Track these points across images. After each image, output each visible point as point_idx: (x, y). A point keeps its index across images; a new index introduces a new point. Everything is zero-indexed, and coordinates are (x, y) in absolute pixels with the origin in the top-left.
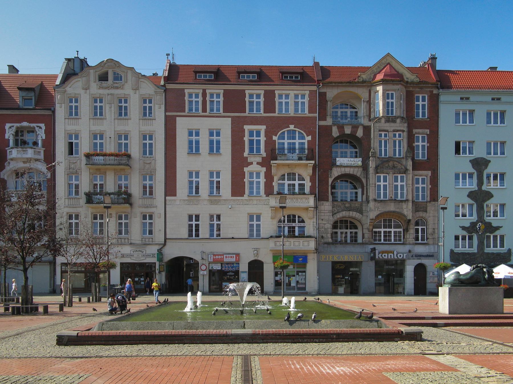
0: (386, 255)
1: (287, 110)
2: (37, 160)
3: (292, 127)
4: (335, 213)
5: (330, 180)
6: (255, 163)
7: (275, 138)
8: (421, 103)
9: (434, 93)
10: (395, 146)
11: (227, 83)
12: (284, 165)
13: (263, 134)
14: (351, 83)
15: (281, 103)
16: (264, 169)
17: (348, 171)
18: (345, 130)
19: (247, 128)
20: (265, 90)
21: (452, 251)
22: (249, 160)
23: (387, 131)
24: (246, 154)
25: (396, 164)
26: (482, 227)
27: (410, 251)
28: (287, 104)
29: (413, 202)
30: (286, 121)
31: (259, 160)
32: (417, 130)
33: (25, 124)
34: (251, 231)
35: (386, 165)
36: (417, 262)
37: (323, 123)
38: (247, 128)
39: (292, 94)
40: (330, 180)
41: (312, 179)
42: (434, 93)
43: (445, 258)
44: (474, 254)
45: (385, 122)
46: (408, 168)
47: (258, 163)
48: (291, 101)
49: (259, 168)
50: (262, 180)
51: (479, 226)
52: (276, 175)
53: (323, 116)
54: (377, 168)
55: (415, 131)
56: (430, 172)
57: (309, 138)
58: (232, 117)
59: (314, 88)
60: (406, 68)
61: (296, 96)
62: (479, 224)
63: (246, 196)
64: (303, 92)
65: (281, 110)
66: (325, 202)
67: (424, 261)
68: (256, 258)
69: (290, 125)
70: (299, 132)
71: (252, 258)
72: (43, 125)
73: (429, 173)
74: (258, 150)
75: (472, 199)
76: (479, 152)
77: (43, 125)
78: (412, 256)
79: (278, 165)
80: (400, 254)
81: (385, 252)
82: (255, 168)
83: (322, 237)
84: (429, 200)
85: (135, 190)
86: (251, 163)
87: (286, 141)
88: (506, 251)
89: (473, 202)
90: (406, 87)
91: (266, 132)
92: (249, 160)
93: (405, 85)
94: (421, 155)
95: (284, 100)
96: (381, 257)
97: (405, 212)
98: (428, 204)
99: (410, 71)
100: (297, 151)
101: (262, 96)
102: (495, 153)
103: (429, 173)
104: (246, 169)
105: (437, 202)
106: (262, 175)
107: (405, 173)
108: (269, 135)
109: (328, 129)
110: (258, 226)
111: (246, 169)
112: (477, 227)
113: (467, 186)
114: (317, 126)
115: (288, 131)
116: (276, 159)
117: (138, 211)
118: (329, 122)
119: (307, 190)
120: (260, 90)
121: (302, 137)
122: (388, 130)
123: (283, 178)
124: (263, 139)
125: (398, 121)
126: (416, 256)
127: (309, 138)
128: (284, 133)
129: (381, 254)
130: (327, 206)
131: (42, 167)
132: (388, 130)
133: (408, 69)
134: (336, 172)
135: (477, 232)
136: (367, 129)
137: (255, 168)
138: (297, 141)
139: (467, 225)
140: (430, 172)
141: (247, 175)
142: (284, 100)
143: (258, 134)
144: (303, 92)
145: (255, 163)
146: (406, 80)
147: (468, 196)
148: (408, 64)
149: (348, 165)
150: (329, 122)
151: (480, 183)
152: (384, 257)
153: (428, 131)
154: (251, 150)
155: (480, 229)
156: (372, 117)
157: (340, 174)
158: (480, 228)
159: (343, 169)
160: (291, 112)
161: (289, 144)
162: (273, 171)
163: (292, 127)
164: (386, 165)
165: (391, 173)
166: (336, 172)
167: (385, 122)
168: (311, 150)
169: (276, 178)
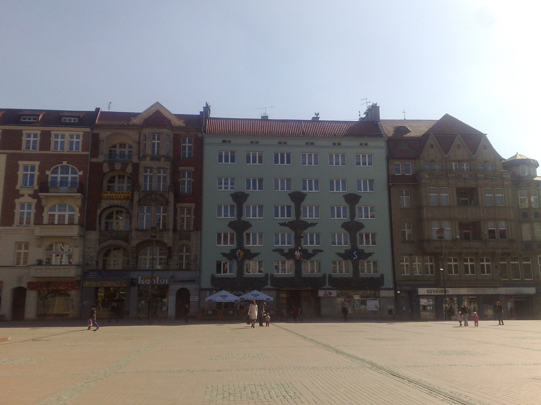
0: (149, 280)
1: (62, 148)
3: (65, 163)
4: (101, 242)
5: (99, 212)
6: (26, 195)
7: (48, 173)
8: (187, 145)
9: (199, 136)
10: (159, 181)
11: (19, 125)
12: (55, 197)
13: (37, 168)
14: (122, 127)
15: (56, 142)
16: (35, 201)
17: (116, 202)
18: (116, 166)
19: (21, 163)
20: (84, 132)
21: (213, 277)
22: (21, 193)
23: (152, 168)
24: (18, 187)
25: (159, 197)
26: (242, 254)
27: (172, 277)
28: (62, 143)
29: (175, 229)
30: (60, 158)
31: (31, 192)
32: (182, 167)
34: (19, 259)
35: (149, 198)
36: (180, 286)
37: (94, 160)
38: (21, 163)
39: (67, 134)
40: (99, 212)
41: (81, 211)
42: (199, 136)
43: (206, 283)
44: (233, 279)
45: (150, 160)
46: (169, 201)
47: (29, 195)
48: (67, 140)
49: (30, 200)
50: (33, 211)
51: (238, 253)
52: (46, 206)
54: (140, 201)
55: (181, 168)
56: (194, 204)
57: (81, 173)
58: (7, 154)
59: (88, 130)
60: (174, 114)
61: (72, 136)
62: (238, 251)
63: (14, 227)
64: (77, 133)
65: (56, 148)
66: (93, 231)
67: (187, 286)
68: (20, 285)
69: (63, 162)
70: (72, 168)
71: (15, 286)
73: (193, 205)
74: (32, 183)
75: (233, 229)
76: (241, 188)
78: (174, 282)
79: (47, 197)
80: (162, 280)
81: (148, 278)
82: (26, 199)
83: (88, 264)
84: (192, 230)
86: (23, 195)
87: (59, 176)
88: (263, 276)
89: (233, 231)
90: (172, 131)
91: (40, 167)
92: (21, 193)
93: (172, 129)
94: (186, 188)
95: (60, 140)
96: (143, 283)
97: (166, 240)
98: (191, 233)
99: (177, 117)
100: (69, 185)
101: (81, 137)
102: (254, 188)
103: (193, 205)
104: (17, 201)
105: (200, 231)
106: (33, 207)
107: (167, 205)
108: (42, 170)
109: (100, 165)
110: (26, 254)
111: (17, 201)
112: (237, 253)
113: (229, 217)
114: (89, 162)
115: (61, 166)
116: (47, 191)
118: (101, 159)
119: (76, 220)
120: (38, 130)
121: (74, 172)
122: (153, 167)
123: (53, 209)
124: (36, 173)
125: (163, 159)
126: (178, 281)
127: (81, 173)
128: (58, 167)
129: (143, 280)
130: (93, 236)
132: (153, 167)
133: (175, 116)
134: (104, 204)
135: (236, 258)
136: (136, 167)
137: (26, 199)
138: (70, 176)
139: (228, 252)
140: (194, 204)
141: (18, 206)
142: (60, 140)
143: (33, 169)
144: (77, 133)
145: (26, 195)
146: (173, 124)
147: (229, 226)
148: (174, 112)
149: (117, 197)
150: (101, 159)
151: (240, 214)
152: (146, 283)
153: (193, 169)
154: (25, 183)
155: (239, 256)
156: (141, 155)
157: (108, 206)
158: (239, 254)
159: (112, 202)
160: (66, 151)
161: (62, 178)
162: (43, 203)
163: (65, 163)
164: (149, 198)
165: (153, 205)
166: (104, 204)
167: (150, 160)
168: (81, 185)
169: (46, 209)
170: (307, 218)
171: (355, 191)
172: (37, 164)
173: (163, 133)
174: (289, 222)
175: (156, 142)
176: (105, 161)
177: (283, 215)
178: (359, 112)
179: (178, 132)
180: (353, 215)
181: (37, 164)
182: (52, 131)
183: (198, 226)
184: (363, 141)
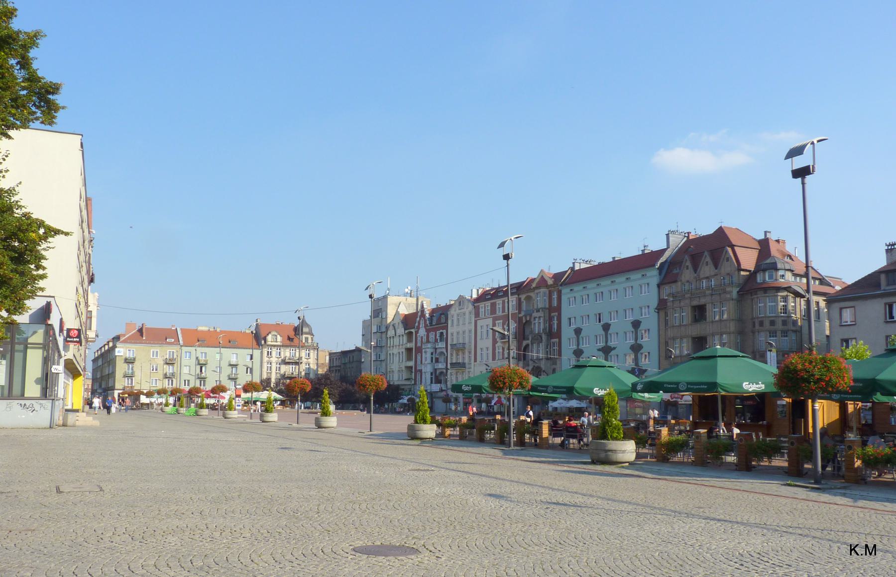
2: (444, 348)
33: (441, 331)
53: (520, 313)
72: (445, 331)
77: (445, 331)
85: (466, 361)
117: (467, 370)
131: (444, 351)
150: (523, 314)
170: (611, 344)
171: (638, 318)
172: (501, 321)
173: (540, 292)
174: (602, 348)
175: (539, 299)
176: (523, 316)
177: (600, 343)
178: (695, 229)
179: (551, 289)
180: (636, 339)
181: (501, 321)
182: (507, 298)
183: (560, 354)
184: (643, 272)
